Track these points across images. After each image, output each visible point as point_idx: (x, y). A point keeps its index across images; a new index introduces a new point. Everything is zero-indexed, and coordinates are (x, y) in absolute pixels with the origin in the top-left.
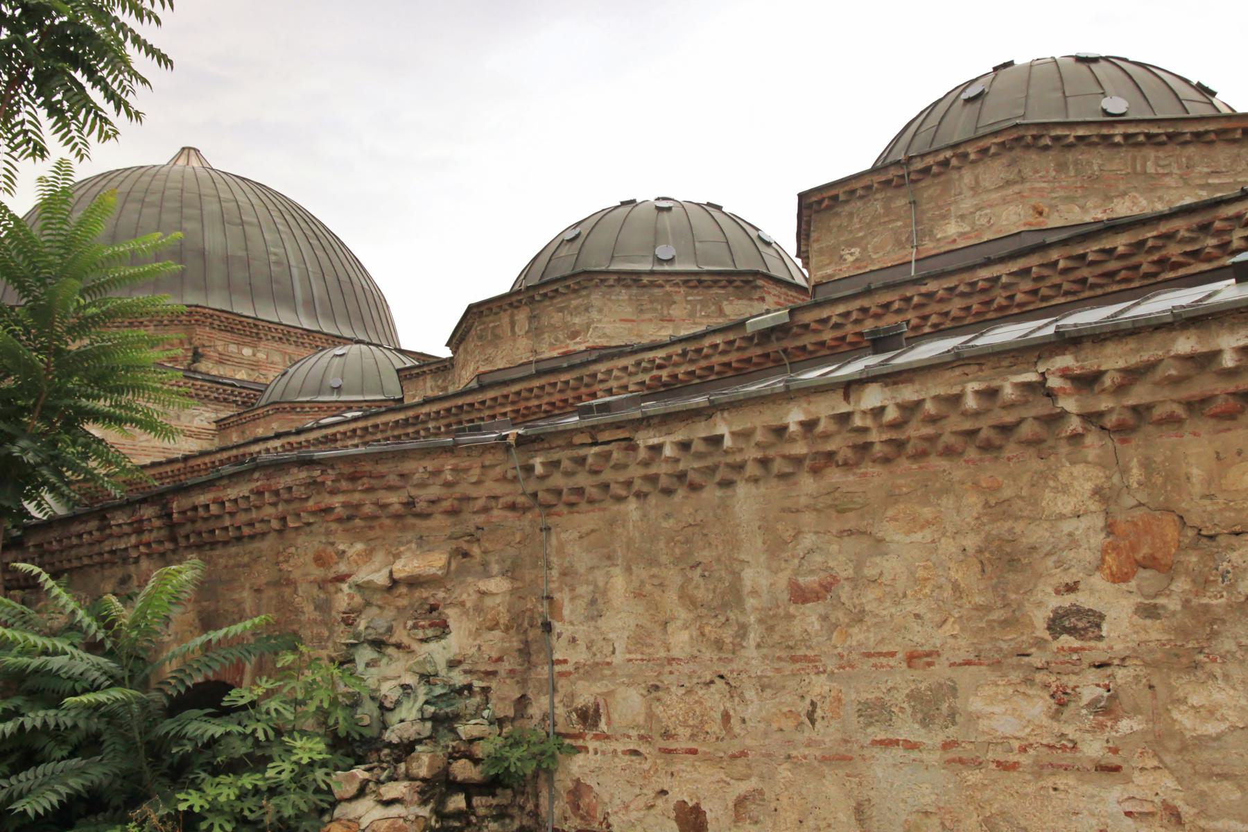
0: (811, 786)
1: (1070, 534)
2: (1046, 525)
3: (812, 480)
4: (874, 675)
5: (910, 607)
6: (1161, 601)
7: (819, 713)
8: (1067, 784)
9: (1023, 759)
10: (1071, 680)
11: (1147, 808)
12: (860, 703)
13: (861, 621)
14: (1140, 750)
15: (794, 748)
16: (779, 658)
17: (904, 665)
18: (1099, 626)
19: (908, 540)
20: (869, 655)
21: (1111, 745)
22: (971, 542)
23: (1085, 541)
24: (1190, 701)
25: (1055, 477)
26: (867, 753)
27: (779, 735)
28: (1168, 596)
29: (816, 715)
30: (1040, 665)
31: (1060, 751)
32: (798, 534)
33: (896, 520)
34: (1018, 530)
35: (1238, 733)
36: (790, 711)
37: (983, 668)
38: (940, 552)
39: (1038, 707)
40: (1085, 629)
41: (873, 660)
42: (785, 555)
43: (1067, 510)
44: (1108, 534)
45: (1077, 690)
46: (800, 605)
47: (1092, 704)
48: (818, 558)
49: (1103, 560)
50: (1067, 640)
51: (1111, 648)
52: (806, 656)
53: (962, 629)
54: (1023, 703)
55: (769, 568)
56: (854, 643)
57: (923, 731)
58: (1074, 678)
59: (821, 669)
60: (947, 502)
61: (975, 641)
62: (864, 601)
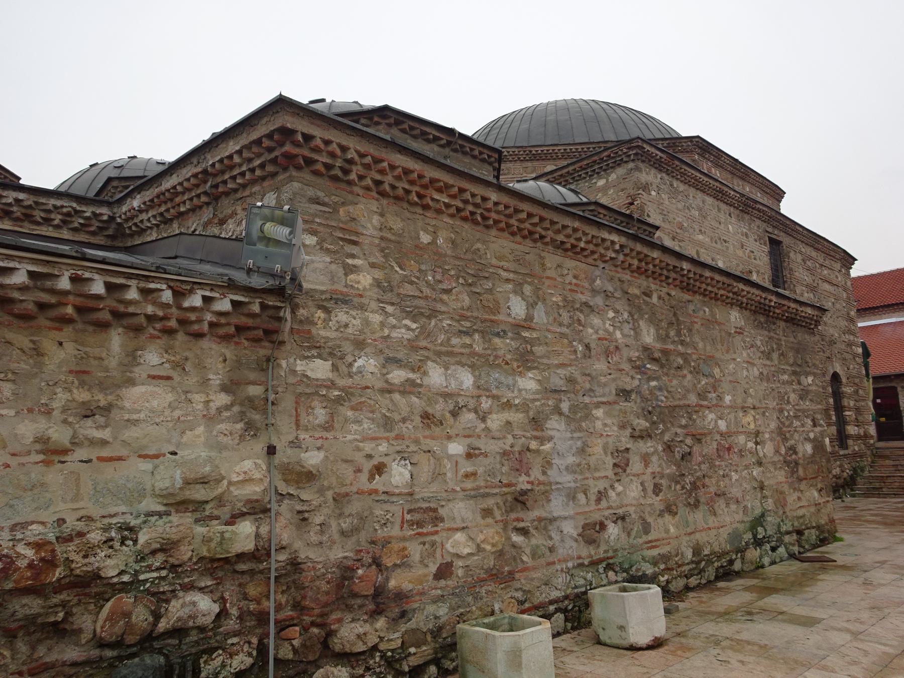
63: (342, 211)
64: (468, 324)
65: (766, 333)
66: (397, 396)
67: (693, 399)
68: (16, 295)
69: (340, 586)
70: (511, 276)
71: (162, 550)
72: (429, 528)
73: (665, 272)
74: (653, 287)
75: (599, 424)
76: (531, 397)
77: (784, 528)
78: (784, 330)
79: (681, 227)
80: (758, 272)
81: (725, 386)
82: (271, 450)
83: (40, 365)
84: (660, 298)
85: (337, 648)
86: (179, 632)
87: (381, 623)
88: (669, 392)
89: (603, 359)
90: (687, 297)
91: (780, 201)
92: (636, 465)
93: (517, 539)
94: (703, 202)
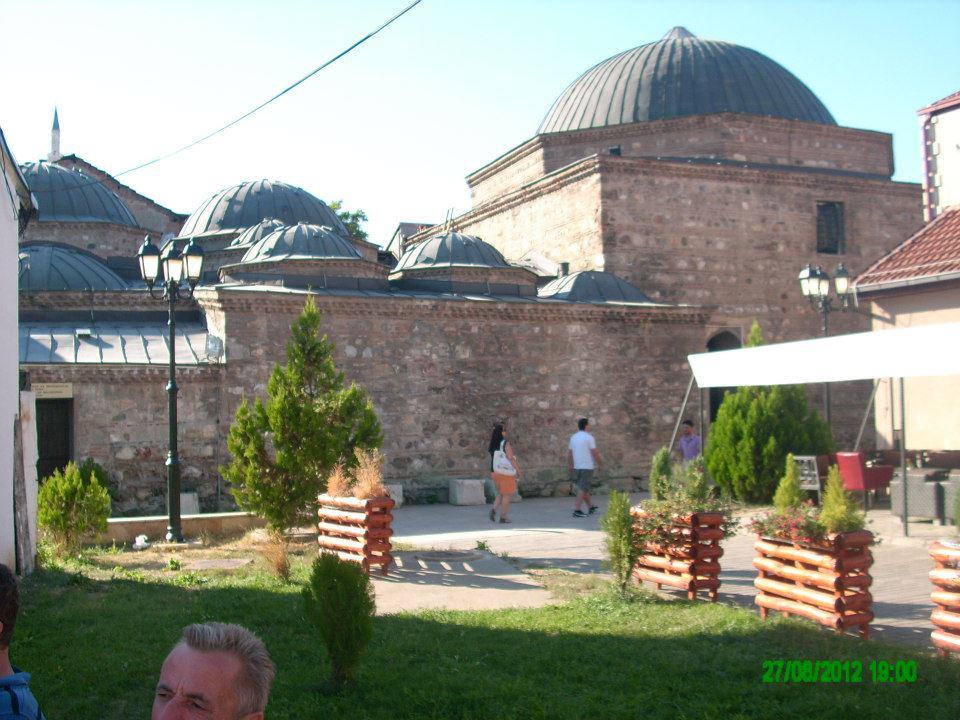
63: (248, 324)
65: (622, 335)
67: (510, 389)
70: (347, 336)
73: (481, 313)
74: (471, 323)
75: (412, 408)
78: (650, 331)
79: (660, 220)
80: (788, 244)
82: (218, 421)
84: (480, 328)
86: (187, 477)
88: (482, 386)
90: (510, 324)
92: (445, 429)
94: (701, 188)
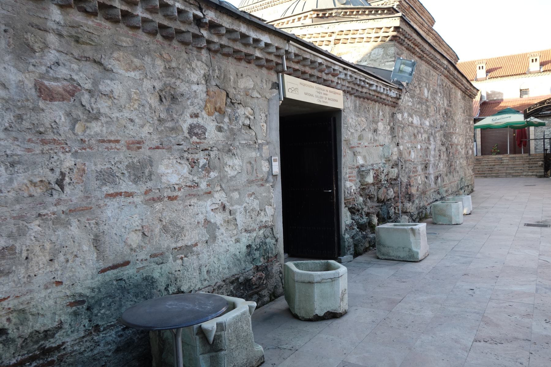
0: (60, 233)
1: (195, 92)
2: (187, 85)
3: (59, 12)
4: (106, 154)
5: (126, 114)
6: (222, 125)
7: (67, 180)
8: (194, 202)
9: (180, 194)
10: (196, 156)
11: (217, 206)
12: (97, 172)
13: (97, 119)
14: (216, 184)
15: (45, 208)
16: (29, 140)
17: (125, 148)
18: (205, 134)
19: (127, 75)
20: (103, 141)
21: (208, 183)
22: (158, 85)
23: (199, 96)
24: (228, 164)
25: (191, 65)
26: (101, 203)
27: (30, 200)
28: (223, 124)
29: (65, 182)
30: (186, 149)
31: (192, 188)
32: (46, 46)
33: (119, 61)
34: (178, 84)
35: (239, 174)
36: (41, 181)
37: (164, 150)
38: (143, 86)
39: (185, 169)
40: (200, 134)
41: (106, 145)
42: (33, 61)
43: (195, 80)
44: (207, 95)
45: (199, 160)
46: (48, 102)
47: (204, 166)
48: (63, 72)
49: (206, 106)
50: (195, 139)
51: (209, 143)
52: (55, 140)
53: (154, 130)
54: (179, 167)
55: (15, 67)
56: (92, 133)
57: (134, 186)
58: (197, 155)
59: (67, 150)
60: (147, 59)
61: (160, 136)
62: (99, 106)
64: (419, 100)
66: (410, 127)
68: (371, 93)
69: (406, 191)
71: (387, 175)
72: (416, 174)
76: (428, 128)
77: (466, 184)
81: (457, 124)
83: (369, 115)
85: (404, 211)
86: (388, 200)
87: (411, 204)
89: (438, 113)
91: (432, 26)
92: (442, 156)
93: (426, 180)
